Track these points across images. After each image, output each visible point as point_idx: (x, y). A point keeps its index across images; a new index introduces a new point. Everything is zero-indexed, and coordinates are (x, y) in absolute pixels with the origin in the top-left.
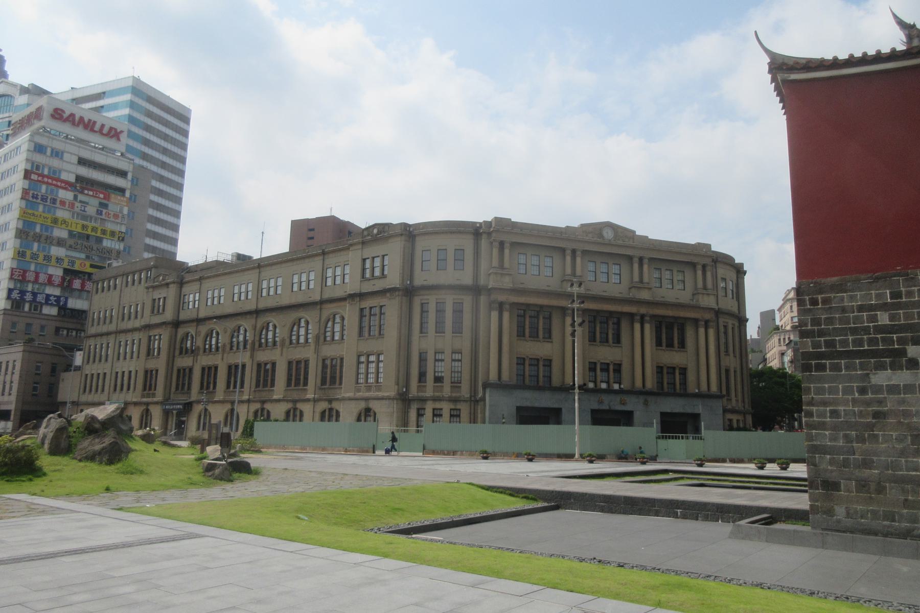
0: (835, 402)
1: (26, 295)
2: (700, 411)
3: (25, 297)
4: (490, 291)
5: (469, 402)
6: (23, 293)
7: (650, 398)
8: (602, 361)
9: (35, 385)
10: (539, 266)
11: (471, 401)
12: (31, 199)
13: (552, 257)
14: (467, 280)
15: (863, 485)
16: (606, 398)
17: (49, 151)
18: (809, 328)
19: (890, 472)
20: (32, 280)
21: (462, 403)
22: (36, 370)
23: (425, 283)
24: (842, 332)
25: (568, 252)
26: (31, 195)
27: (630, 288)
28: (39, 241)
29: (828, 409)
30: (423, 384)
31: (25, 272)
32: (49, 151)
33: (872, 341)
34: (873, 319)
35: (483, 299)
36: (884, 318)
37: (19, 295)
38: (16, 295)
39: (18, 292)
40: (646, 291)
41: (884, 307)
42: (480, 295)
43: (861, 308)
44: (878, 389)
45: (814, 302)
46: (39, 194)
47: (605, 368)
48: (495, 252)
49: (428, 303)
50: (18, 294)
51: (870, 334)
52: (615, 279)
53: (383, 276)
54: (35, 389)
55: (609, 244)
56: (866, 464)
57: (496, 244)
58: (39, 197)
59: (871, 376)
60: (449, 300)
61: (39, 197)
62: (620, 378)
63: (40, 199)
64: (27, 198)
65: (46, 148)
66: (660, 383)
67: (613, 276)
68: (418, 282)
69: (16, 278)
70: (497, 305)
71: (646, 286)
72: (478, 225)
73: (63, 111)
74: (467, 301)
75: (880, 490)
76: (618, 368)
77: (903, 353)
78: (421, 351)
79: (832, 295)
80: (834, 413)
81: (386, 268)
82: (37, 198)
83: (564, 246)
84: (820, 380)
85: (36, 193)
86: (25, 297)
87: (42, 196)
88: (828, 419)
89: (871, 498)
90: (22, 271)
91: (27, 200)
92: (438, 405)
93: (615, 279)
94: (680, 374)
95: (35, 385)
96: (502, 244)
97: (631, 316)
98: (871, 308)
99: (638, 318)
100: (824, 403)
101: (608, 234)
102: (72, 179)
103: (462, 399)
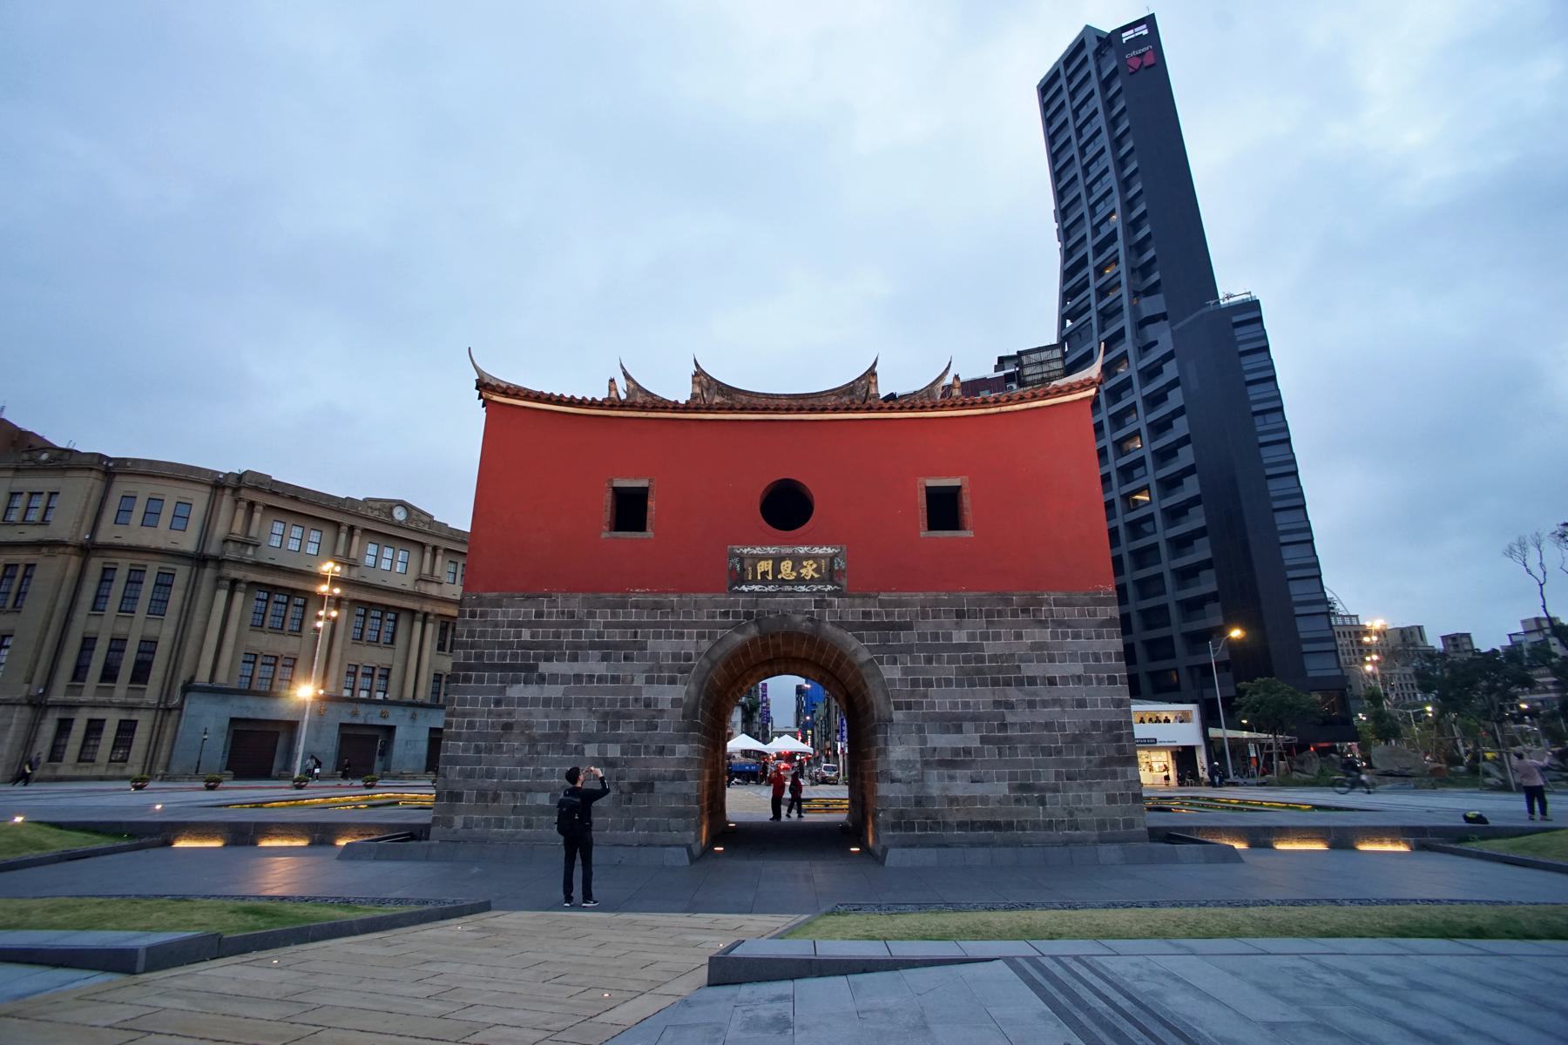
0: (473, 714)
4: (219, 562)
5: (154, 711)
7: (419, 711)
10: (301, 540)
11: (158, 709)
13: (322, 531)
14: (188, 543)
15: (482, 795)
16: (363, 710)
18: (464, 639)
19: (507, 780)
23: (117, 541)
24: (488, 645)
25: (344, 528)
27: (417, 580)
29: (466, 720)
30: (78, 684)
33: (514, 656)
34: (518, 635)
35: (208, 573)
36: (526, 635)
40: (435, 585)
41: (529, 624)
42: (205, 567)
43: (511, 624)
44: (510, 702)
45: (473, 615)
48: (241, 514)
49: (115, 569)
51: (513, 649)
52: (399, 567)
53: (44, 522)
55: (399, 525)
56: (490, 774)
57: (244, 504)
59: (507, 689)
60: (153, 568)
62: (387, 686)
66: (436, 693)
67: (399, 564)
68: (103, 537)
70: (228, 583)
71: (436, 579)
72: (221, 476)
74: (182, 572)
75: (496, 798)
76: (386, 676)
77: (535, 668)
78: (87, 636)
79: (489, 609)
80: (471, 725)
81: (50, 511)
83: (339, 521)
84: (465, 691)
88: (465, 730)
89: (487, 806)
92: (98, 714)
93: (399, 567)
96: (252, 505)
97: (413, 612)
98: (519, 625)
99: (421, 616)
100: (464, 715)
101: (399, 515)
103: (143, 706)
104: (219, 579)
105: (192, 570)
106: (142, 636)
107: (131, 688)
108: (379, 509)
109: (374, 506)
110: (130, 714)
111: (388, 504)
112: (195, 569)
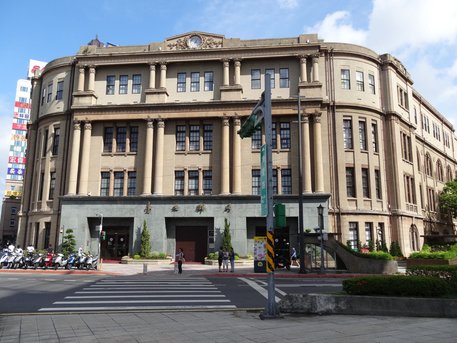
1: (18, 171)
3: (18, 172)
6: (17, 170)
12: (19, 117)
20: (21, 162)
26: (19, 115)
31: (17, 158)
37: (15, 171)
38: (13, 171)
39: (14, 169)
46: (24, 114)
50: (14, 171)
58: (24, 116)
61: (24, 116)
63: (24, 117)
64: (17, 117)
69: (12, 162)
73: (39, 67)
82: (23, 117)
85: (22, 114)
86: (18, 172)
87: (25, 115)
90: (15, 158)
91: (17, 118)
94: (282, 176)
105: (67, 121)
108: (176, 45)
109: (172, 44)
111: (182, 39)
112: (69, 121)
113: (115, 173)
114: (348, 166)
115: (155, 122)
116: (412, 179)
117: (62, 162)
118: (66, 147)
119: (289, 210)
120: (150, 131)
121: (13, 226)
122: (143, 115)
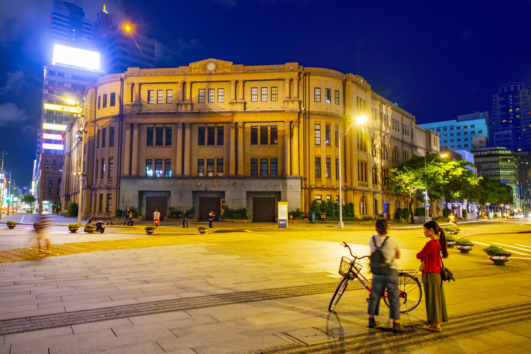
2: (281, 190)
8: (208, 158)
9: (50, 189)
17: (57, 74)
21: (112, 189)
22: (50, 182)
28: (56, 119)
32: (57, 74)
47: (210, 163)
54: (50, 191)
65: (55, 72)
95: (50, 189)
102: (69, 86)
104: (126, 124)
105: (120, 123)
106: (109, 157)
107: (109, 180)
110: (109, 192)
112: (121, 122)
113: (156, 160)
114: (316, 156)
115: (184, 124)
116: (365, 164)
117: (117, 152)
118: (120, 141)
119: (275, 187)
120: (180, 131)
121: (51, 194)
122: (176, 120)
